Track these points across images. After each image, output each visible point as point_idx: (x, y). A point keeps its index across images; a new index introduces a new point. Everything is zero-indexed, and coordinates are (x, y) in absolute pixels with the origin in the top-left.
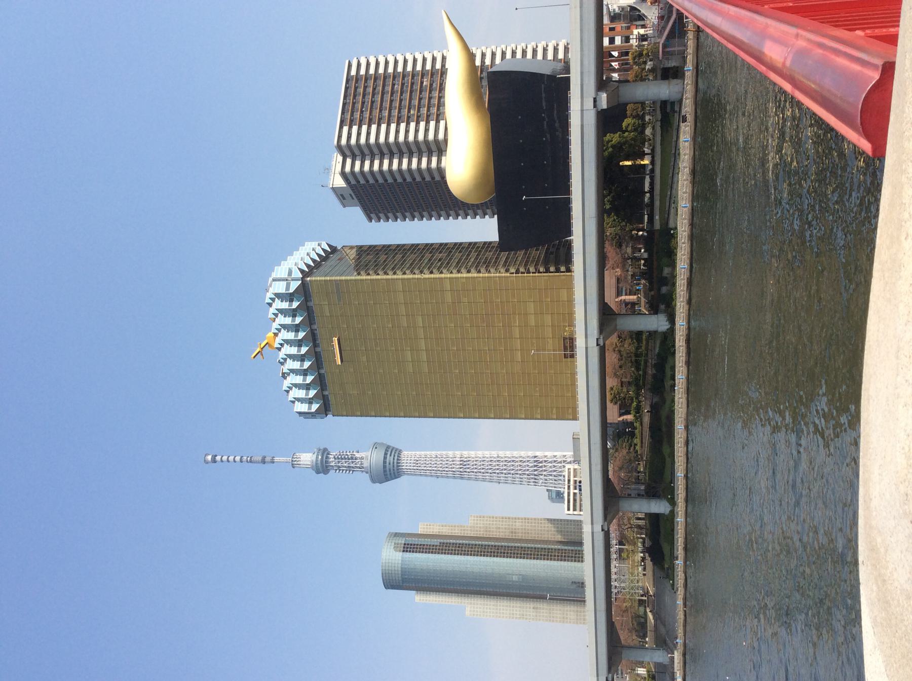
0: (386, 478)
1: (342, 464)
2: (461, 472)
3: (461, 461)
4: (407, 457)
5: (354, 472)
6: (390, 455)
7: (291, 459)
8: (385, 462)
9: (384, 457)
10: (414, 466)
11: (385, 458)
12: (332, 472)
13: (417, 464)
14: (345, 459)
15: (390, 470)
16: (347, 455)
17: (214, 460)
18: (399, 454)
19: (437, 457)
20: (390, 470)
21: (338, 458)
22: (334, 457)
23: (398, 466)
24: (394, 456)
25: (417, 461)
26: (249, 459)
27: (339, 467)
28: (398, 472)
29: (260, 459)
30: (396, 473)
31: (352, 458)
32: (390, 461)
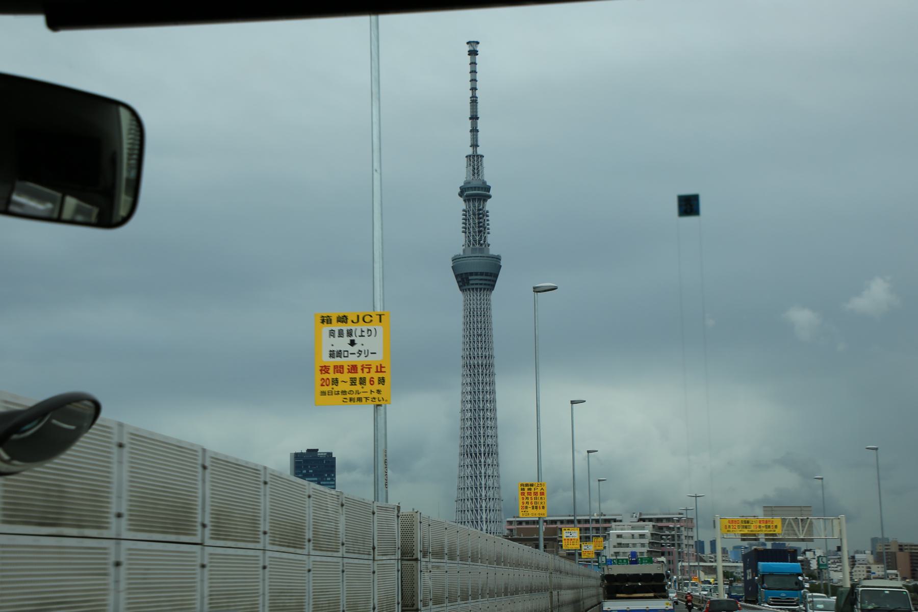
5: (464, 234)
8: (476, 274)
21: (479, 214)
22: (480, 210)
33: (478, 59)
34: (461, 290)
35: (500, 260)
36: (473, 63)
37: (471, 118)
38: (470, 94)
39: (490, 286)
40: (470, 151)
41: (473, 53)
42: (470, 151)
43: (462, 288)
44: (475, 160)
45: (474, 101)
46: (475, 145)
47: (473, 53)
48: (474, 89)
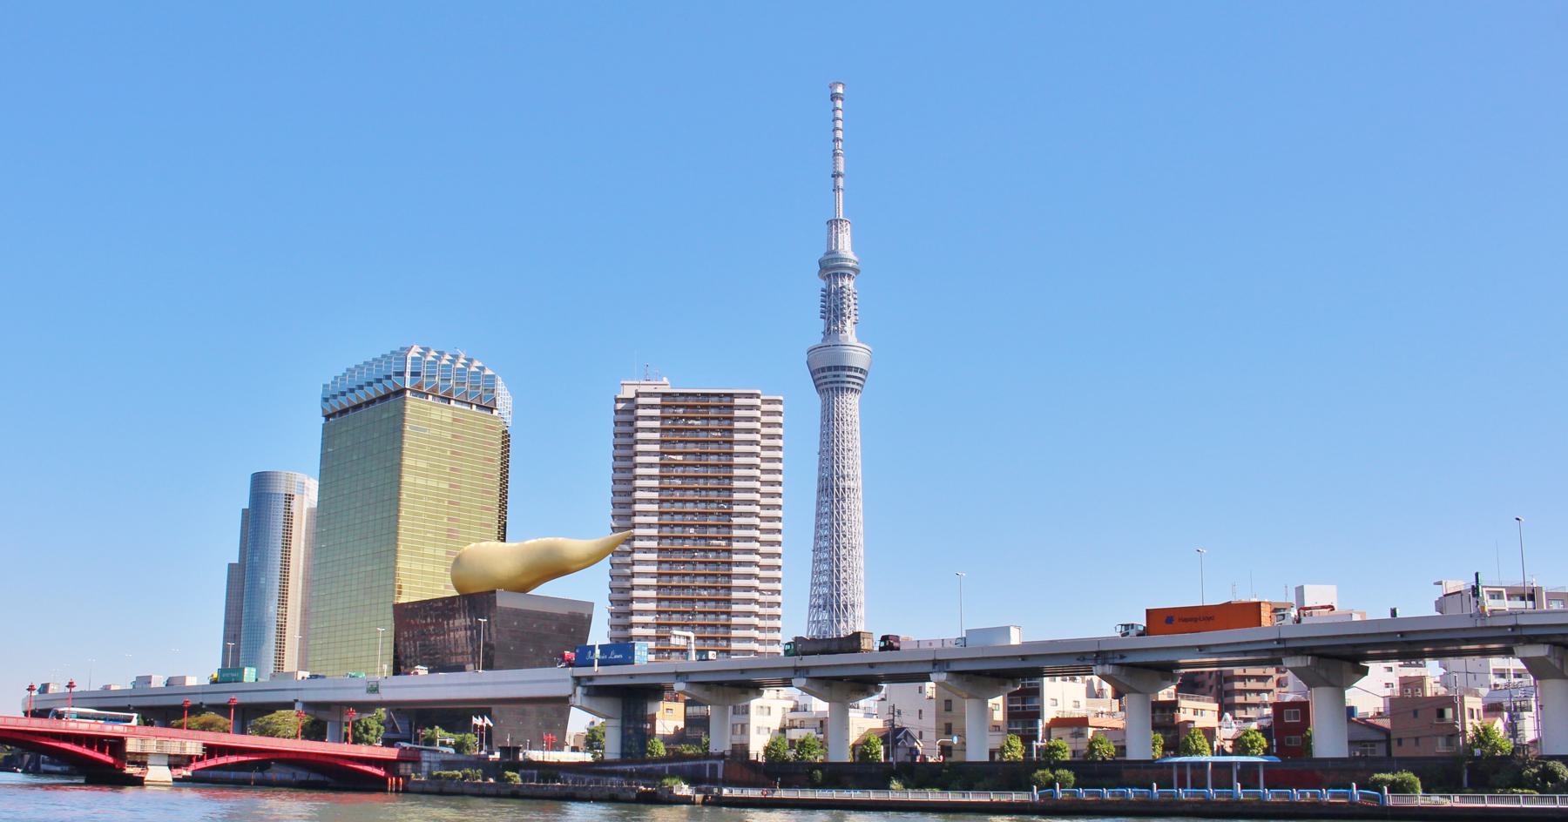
2: (827, 490)
7: (841, 217)
12: (823, 284)
13: (837, 420)
15: (825, 377)
16: (849, 306)
17: (834, 97)
19: (849, 450)
20: (825, 377)
23: (832, 389)
25: (842, 420)
27: (829, 296)
28: (827, 389)
29: (841, 169)
30: (821, 388)
31: (844, 315)
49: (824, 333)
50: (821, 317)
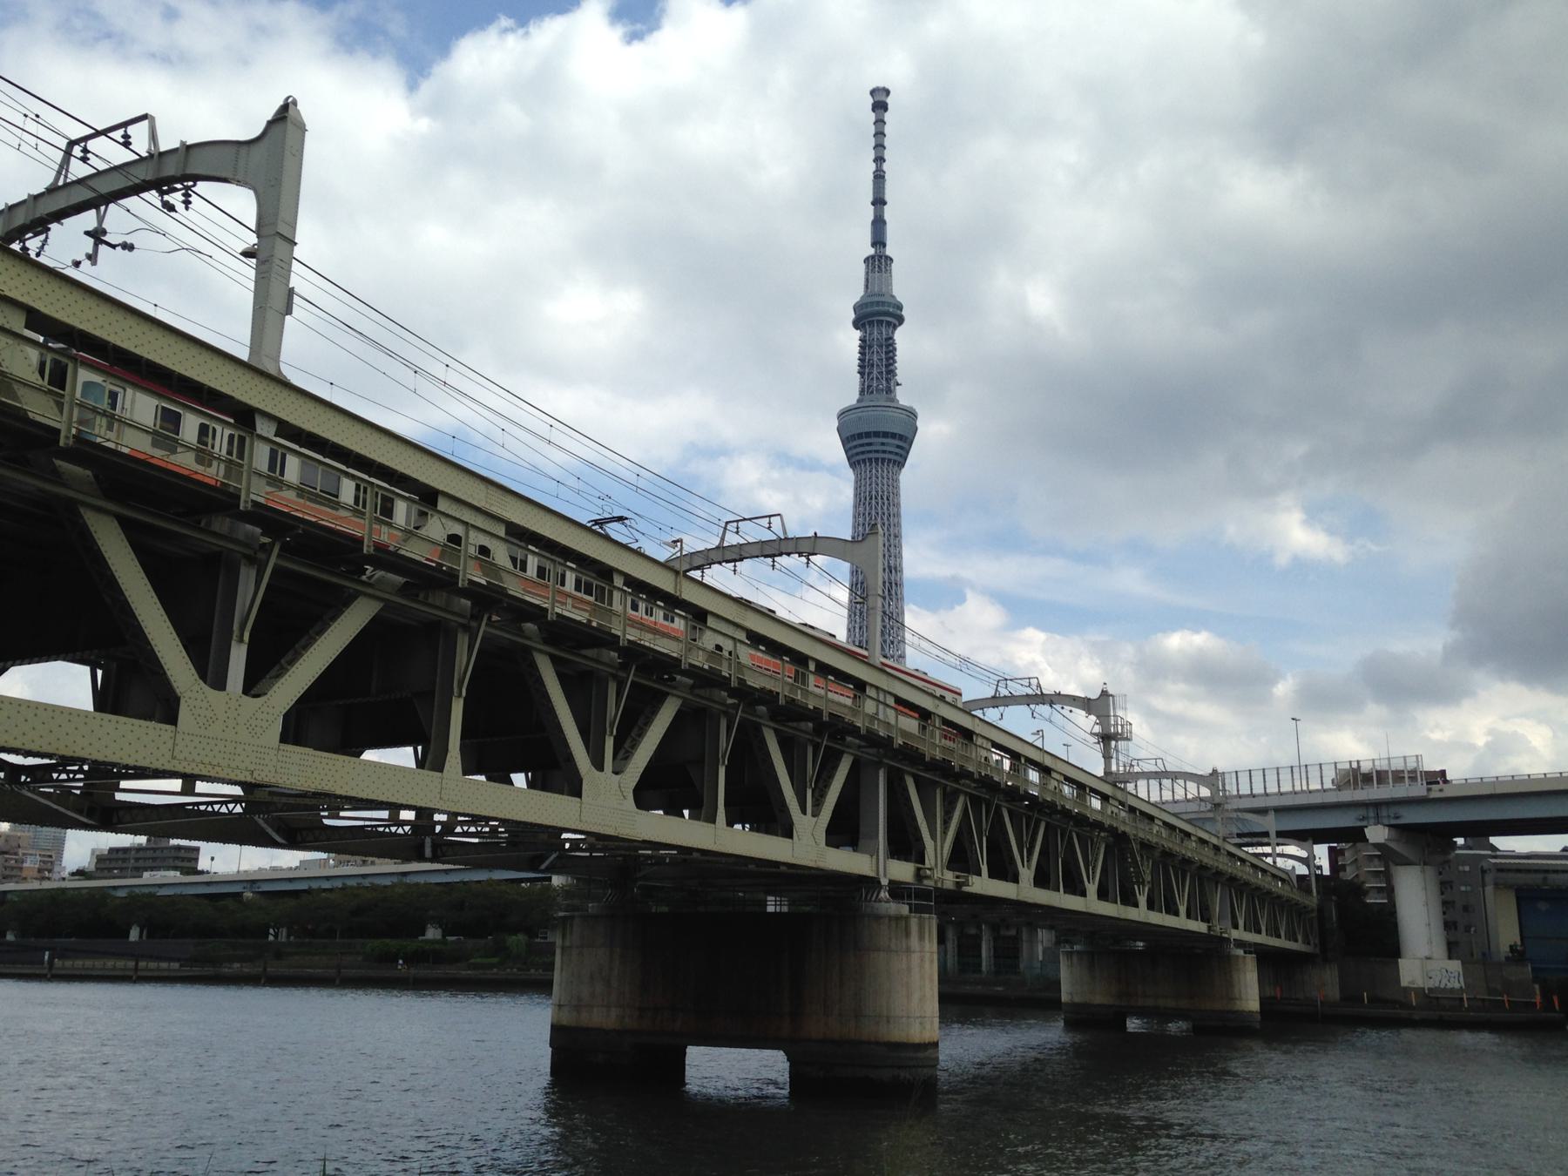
0: (848, 438)
1: (878, 352)
3: (891, 583)
4: (893, 480)
6: (898, 447)
8: (886, 435)
9: (896, 434)
10: (877, 492)
11: (893, 436)
12: (858, 334)
13: (882, 498)
14: (887, 359)
15: (870, 444)
18: (895, 461)
19: (896, 536)
20: (870, 444)
21: (888, 346)
24: (897, 454)
26: (882, 173)
27: (870, 347)
28: (859, 462)
32: (888, 444)
33: (887, 117)
34: (851, 465)
35: (916, 417)
36: (880, 122)
37: (873, 204)
38: (873, 167)
39: (900, 460)
40: (872, 251)
41: (880, 106)
42: (872, 251)
43: (853, 460)
44: (878, 263)
45: (879, 177)
46: (879, 241)
47: (880, 106)
48: (879, 160)
49: (862, 392)
50: (859, 372)
